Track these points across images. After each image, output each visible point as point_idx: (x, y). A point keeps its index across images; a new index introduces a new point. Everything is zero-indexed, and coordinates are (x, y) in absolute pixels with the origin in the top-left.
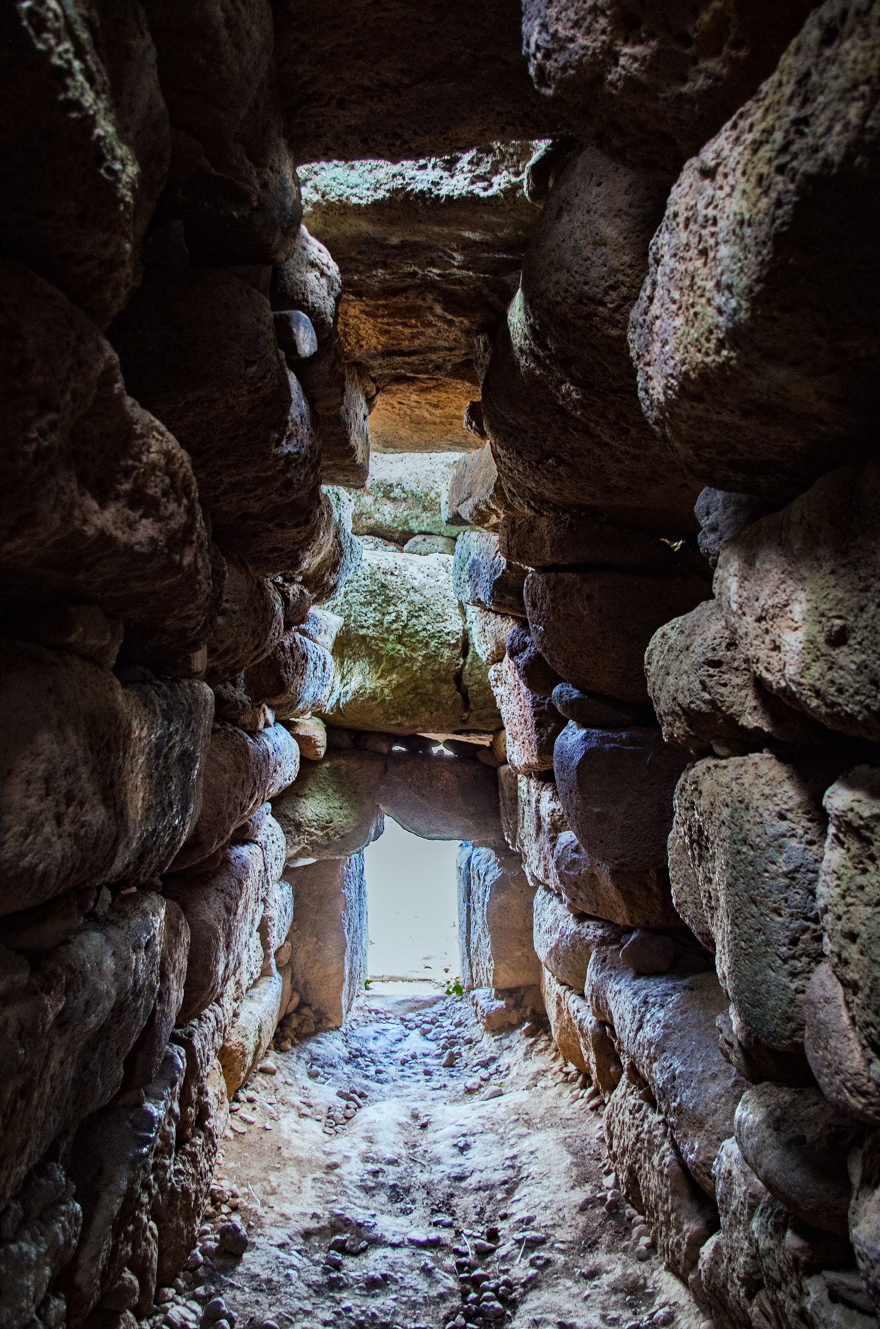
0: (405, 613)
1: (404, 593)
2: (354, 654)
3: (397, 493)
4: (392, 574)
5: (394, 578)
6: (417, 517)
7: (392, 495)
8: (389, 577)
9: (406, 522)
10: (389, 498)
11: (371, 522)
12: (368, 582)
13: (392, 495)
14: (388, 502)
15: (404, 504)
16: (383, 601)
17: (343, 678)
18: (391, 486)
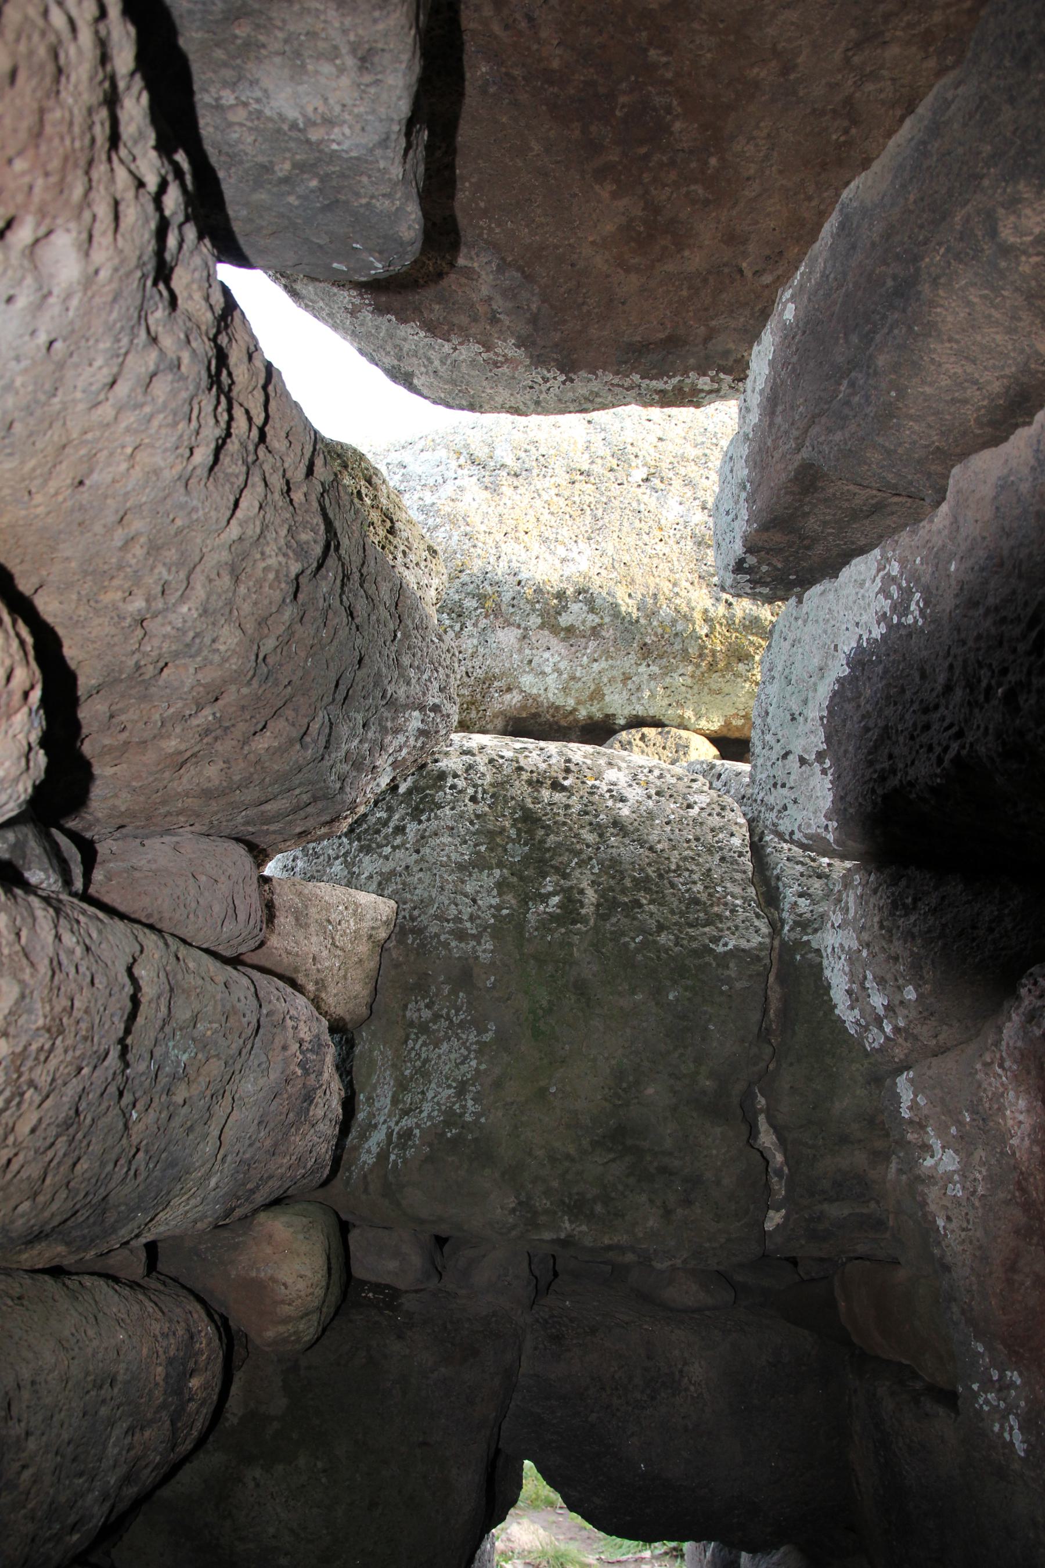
0: (591, 896)
1: (591, 838)
2: (437, 1017)
3: (576, 614)
4: (556, 786)
5: (559, 797)
6: (627, 678)
7: (564, 620)
8: (545, 793)
9: (597, 695)
10: (555, 629)
11: (513, 699)
12: (483, 808)
13: (564, 620)
14: (554, 642)
15: (592, 644)
16: (526, 859)
17: (402, 1085)
18: (561, 595)
